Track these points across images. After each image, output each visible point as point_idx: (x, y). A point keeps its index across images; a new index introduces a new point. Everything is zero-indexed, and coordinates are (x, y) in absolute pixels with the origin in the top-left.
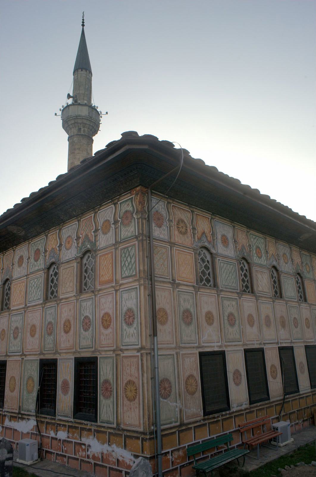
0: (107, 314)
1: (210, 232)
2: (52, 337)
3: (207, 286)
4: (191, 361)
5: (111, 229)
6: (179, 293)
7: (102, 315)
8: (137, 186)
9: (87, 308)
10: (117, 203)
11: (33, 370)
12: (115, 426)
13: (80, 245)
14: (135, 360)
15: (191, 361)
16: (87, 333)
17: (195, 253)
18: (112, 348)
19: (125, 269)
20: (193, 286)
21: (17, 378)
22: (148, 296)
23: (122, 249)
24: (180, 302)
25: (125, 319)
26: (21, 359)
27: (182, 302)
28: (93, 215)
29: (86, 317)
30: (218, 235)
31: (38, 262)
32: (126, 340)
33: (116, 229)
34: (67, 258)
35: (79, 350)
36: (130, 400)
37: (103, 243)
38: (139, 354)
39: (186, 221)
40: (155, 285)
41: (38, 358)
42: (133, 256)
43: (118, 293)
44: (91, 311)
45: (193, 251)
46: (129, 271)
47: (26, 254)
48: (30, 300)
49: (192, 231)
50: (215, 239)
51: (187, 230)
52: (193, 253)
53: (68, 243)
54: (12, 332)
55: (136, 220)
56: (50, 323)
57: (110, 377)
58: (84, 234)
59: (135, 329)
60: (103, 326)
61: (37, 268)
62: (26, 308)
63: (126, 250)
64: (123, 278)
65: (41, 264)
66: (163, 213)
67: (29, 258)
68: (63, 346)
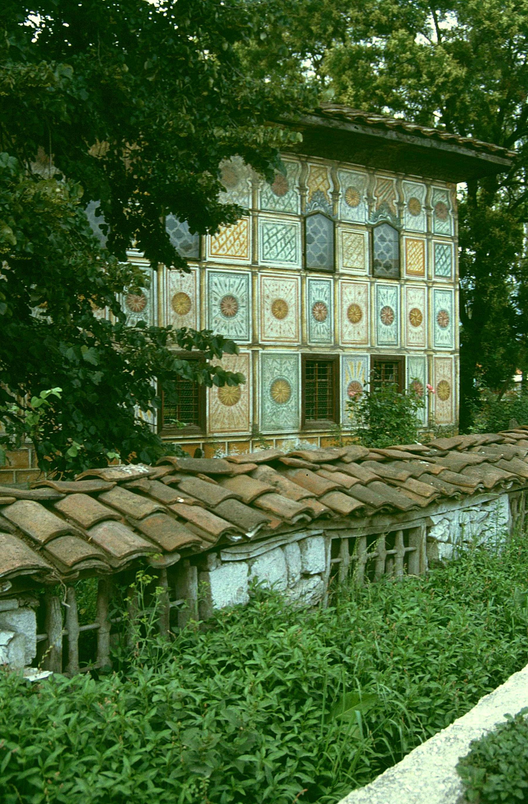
0: (415, 310)
7: (409, 310)
11: (287, 369)
13: (374, 209)
14: (449, 362)
16: (389, 327)
23: (435, 244)
26: (250, 352)
28: (395, 180)
32: (440, 341)
33: (428, 216)
35: (377, 346)
36: (443, 399)
37: (410, 223)
38: (452, 356)
44: (394, 302)
48: (268, 256)
64: (436, 276)
68: (346, 338)
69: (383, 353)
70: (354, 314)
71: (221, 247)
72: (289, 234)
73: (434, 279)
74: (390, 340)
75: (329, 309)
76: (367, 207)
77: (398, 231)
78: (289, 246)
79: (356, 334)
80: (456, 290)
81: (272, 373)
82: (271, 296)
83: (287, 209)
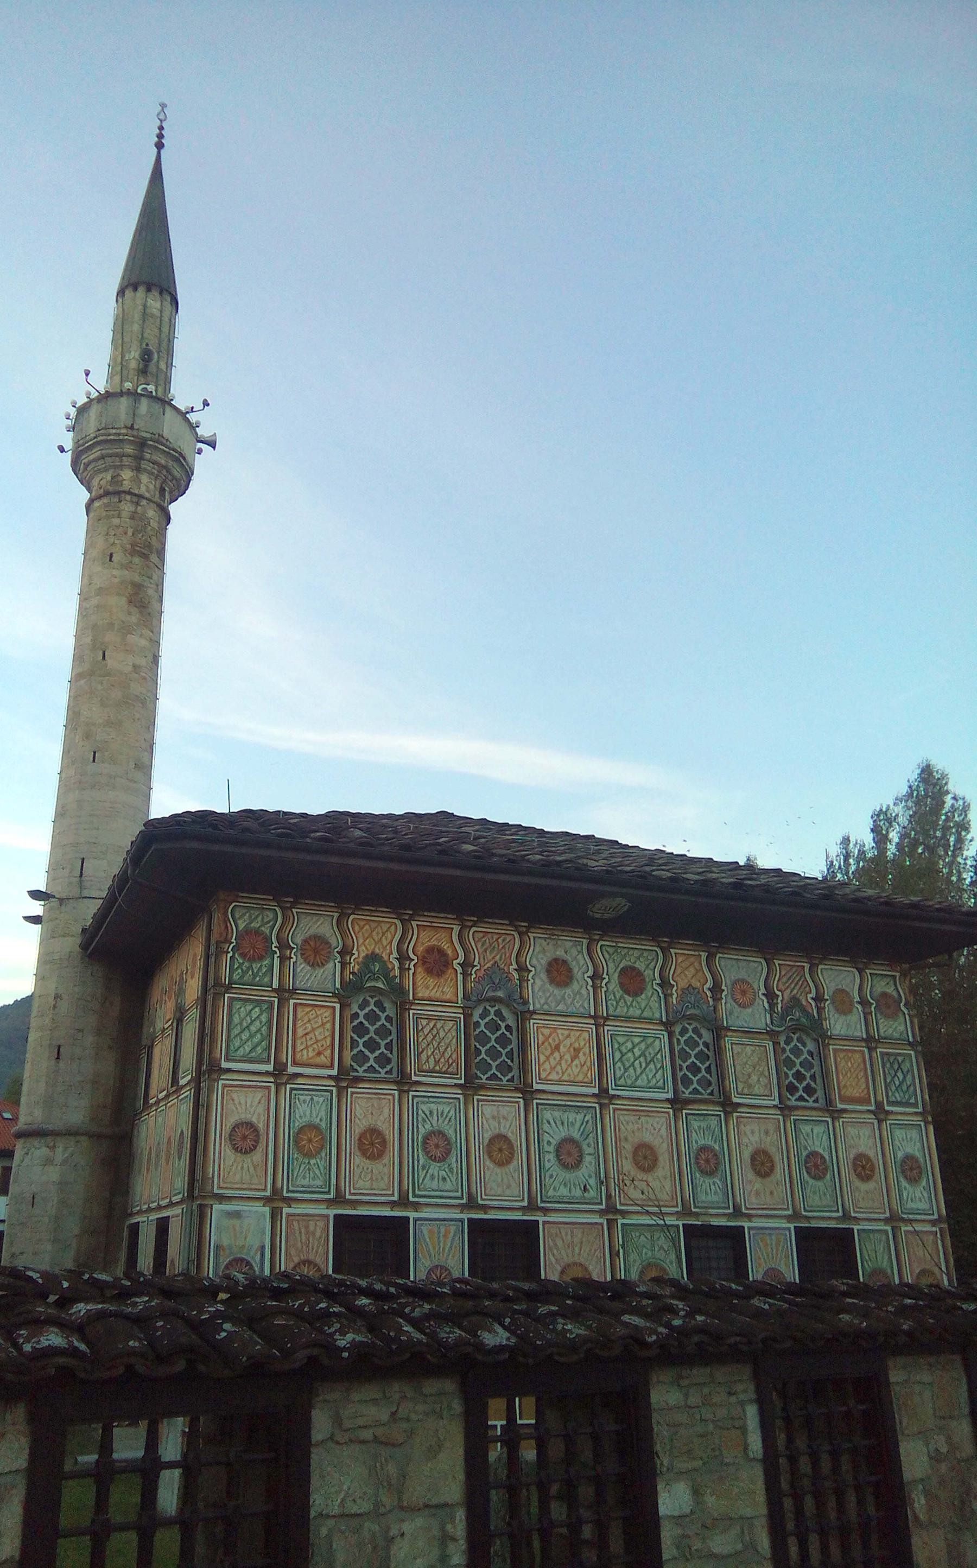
5: (855, 1010)
7: (852, 1156)
9: (816, 1137)
16: (820, 1183)
19: (893, 1088)
25: (903, 1172)
28: (807, 966)
29: (814, 1154)
31: (639, 999)
32: (911, 1205)
34: (739, 1023)
37: (838, 1027)
42: (908, 1071)
44: (825, 1143)
46: (902, 1094)
47: (582, 962)
48: (622, 1082)
56: (703, 1149)
64: (891, 1103)
69: (814, 1224)
70: (762, 1164)
71: (553, 1068)
72: (651, 1050)
74: (824, 1203)
75: (721, 1157)
76: (766, 1005)
77: (823, 1038)
78: (652, 1066)
79: (768, 1193)
80: (926, 1123)
81: (640, 1254)
82: (630, 1138)
83: (645, 1014)
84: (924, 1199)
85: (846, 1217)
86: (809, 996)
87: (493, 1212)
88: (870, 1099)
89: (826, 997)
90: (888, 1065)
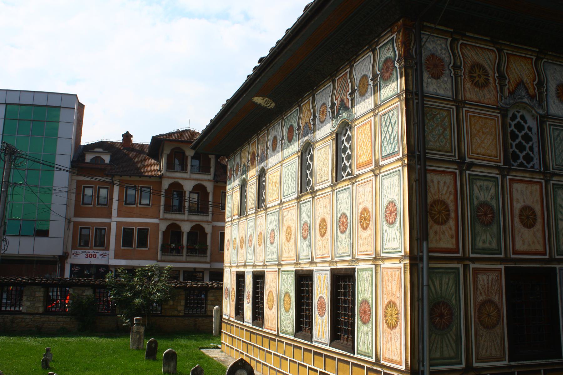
0: (365, 210)
1: (534, 81)
2: (307, 242)
3: (527, 167)
4: (490, 279)
5: (369, 87)
6: (471, 177)
7: (360, 211)
8: (399, 20)
10: (375, 49)
12: (373, 360)
15: (490, 279)
17: (504, 116)
18: (371, 257)
20: (497, 167)
21: (275, 294)
22: (416, 181)
24: (473, 191)
25: (386, 216)
26: (277, 270)
27: (476, 191)
28: (348, 70)
29: (343, 215)
30: (549, 84)
33: (374, 86)
39: (487, 67)
40: (425, 165)
41: (293, 268)
43: (378, 179)
45: (499, 113)
46: (390, 146)
48: (285, 194)
49: (497, 82)
50: (543, 92)
51: (488, 80)
52: (499, 115)
53: (323, 114)
54: (269, 236)
55: (398, 70)
56: (305, 223)
57: (369, 295)
58: (339, 100)
59: (397, 230)
60: (362, 226)
61: (290, 153)
62: (282, 203)
63: (387, 116)
65: (295, 147)
66: (444, 56)
67: (283, 138)
73: (381, 163)
80: (403, 166)
84: (396, 238)
85: (354, 260)
86: (348, 93)
87: (257, 267)
88: (372, 159)
89: (356, 88)
90: (384, 124)
